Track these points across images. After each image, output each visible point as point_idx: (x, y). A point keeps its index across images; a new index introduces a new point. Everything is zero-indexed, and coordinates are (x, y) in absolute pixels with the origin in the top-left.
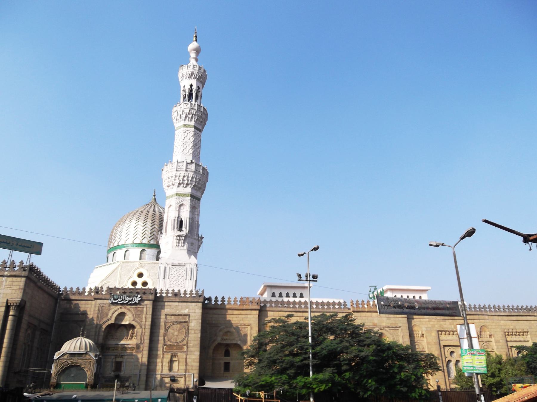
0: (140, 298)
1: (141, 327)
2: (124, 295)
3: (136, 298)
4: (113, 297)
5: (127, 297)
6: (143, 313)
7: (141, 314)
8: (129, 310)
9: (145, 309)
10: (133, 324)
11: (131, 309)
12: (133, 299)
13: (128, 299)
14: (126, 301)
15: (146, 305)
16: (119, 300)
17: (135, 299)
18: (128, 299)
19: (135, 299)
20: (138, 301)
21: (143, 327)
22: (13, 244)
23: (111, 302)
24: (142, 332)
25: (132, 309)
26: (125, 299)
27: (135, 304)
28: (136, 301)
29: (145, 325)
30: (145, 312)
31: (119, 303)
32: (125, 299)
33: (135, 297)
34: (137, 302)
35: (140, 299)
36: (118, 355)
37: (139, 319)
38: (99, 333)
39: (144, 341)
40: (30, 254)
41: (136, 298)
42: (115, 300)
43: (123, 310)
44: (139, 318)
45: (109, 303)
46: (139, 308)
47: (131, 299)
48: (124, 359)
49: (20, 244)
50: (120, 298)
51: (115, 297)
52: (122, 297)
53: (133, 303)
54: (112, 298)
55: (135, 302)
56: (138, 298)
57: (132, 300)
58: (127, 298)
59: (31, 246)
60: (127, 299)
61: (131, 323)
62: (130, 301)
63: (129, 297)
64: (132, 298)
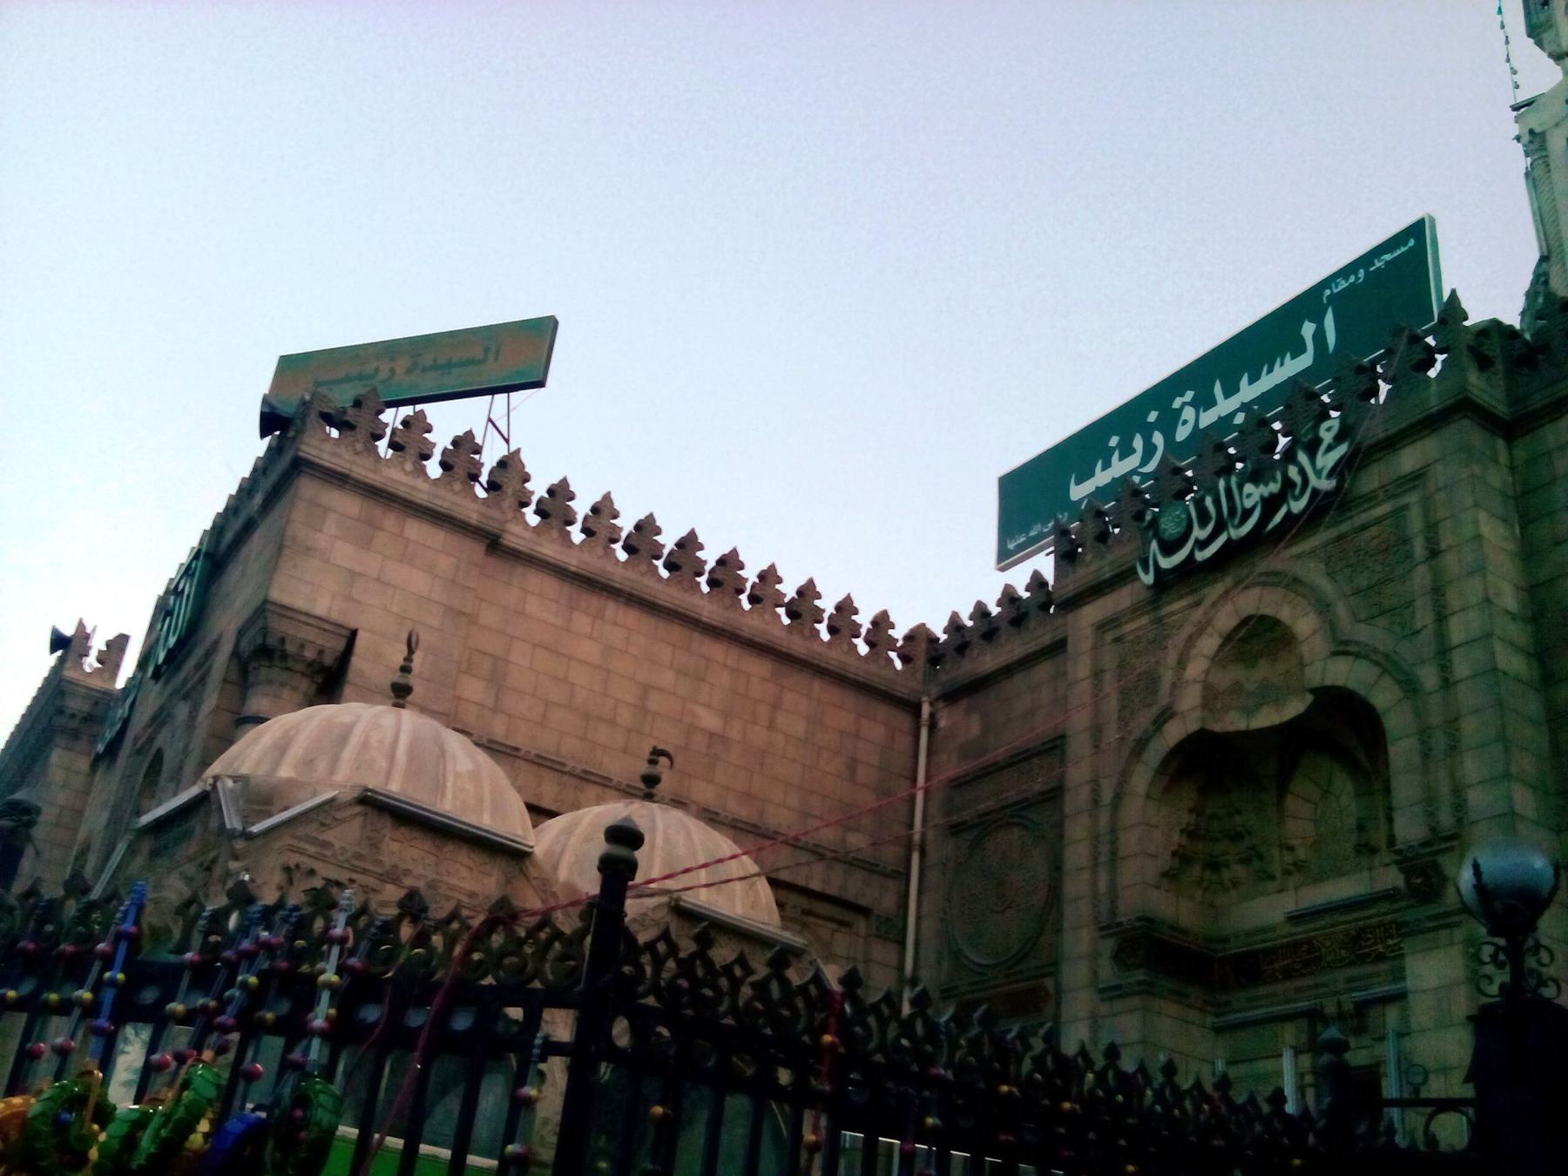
0: (1339, 439)
1: (1410, 687)
2: (1222, 484)
3: (1312, 456)
4: (1157, 535)
5: (1240, 487)
6: (1409, 556)
7: (1388, 580)
8: (1295, 584)
9: (1415, 522)
10: (1340, 683)
11: (1298, 569)
12: (1293, 472)
13: (1253, 494)
14: (1247, 513)
15: (1417, 478)
16: (1199, 533)
17: (1302, 472)
18: (1253, 494)
19: (1302, 472)
20: (1330, 475)
21: (1429, 677)
22: (393, 371)
23: (1148, 579)
24: (1424, 733)
25: (1314, 573)
26: (1232, 510)
27: (1322, 507)
28: (1314, 481)
29: (1443, 652)
30: (1419, 548)
31: (1201, 556)
32: (1232, 510)
33: (1302, 457)
34: (1326, 485)
35: (1342, 449)
36: (1330, 1008)
37: (1382, 622)
38: (1114, 842)
39: (1459, 805)
40: (501, 398)
41: (1312, 456)
42: (1169, 548)
43: (1250, 602)
44: (1382, 614)
45: (1144, 595)
46: (1367, 535)
47: (1274, 487)
48: (1382, 1039)
49: (427, 360)
50: (1203, 522)
51: (1170, 528)
52: (1209, 501)
53: (1297, 506)
54: (1154, 545)
55: (1315, 492)
56: (1330, 448)
57: (1288, 484)
58: (1249, 488)
59: (487, 350)
60: (1248, 504)
61: (1328, 682)
62: (1270, 505)
63: (1256, 477)
64: (1279, 476)
